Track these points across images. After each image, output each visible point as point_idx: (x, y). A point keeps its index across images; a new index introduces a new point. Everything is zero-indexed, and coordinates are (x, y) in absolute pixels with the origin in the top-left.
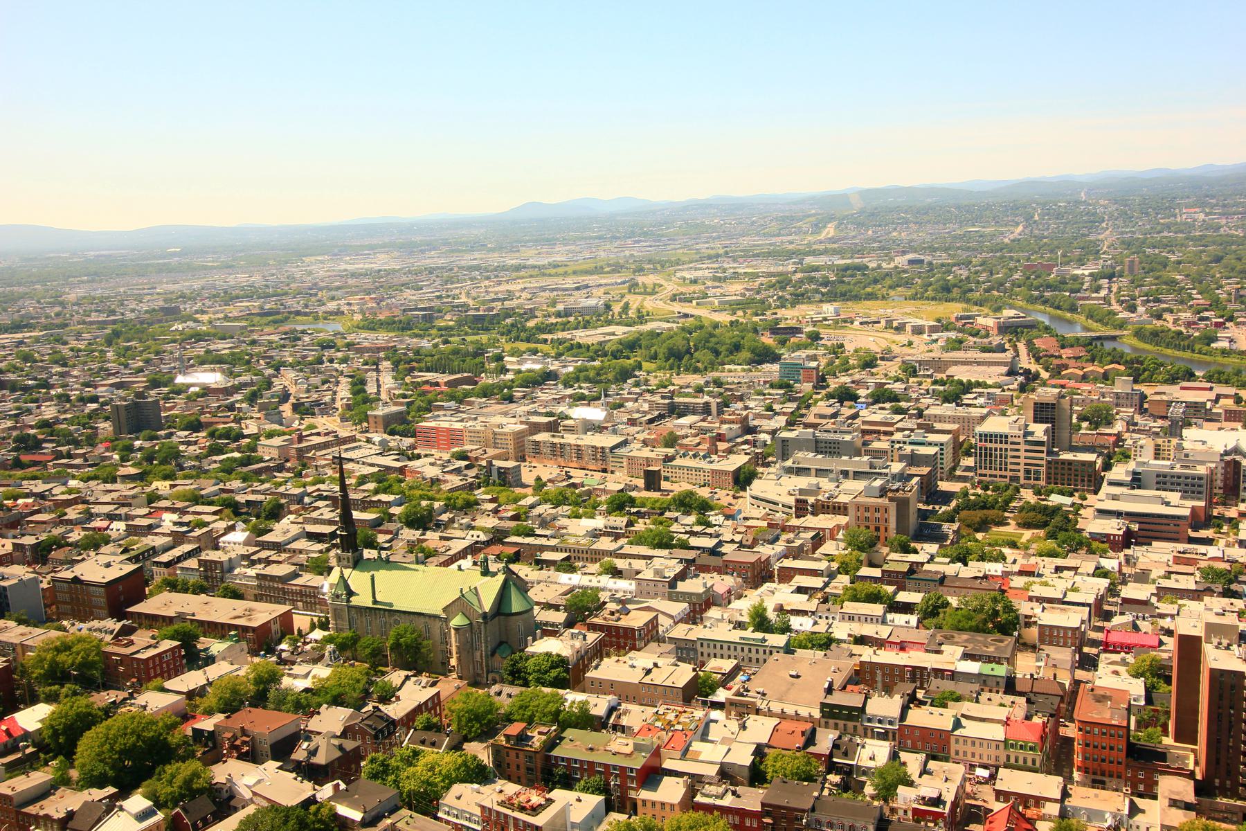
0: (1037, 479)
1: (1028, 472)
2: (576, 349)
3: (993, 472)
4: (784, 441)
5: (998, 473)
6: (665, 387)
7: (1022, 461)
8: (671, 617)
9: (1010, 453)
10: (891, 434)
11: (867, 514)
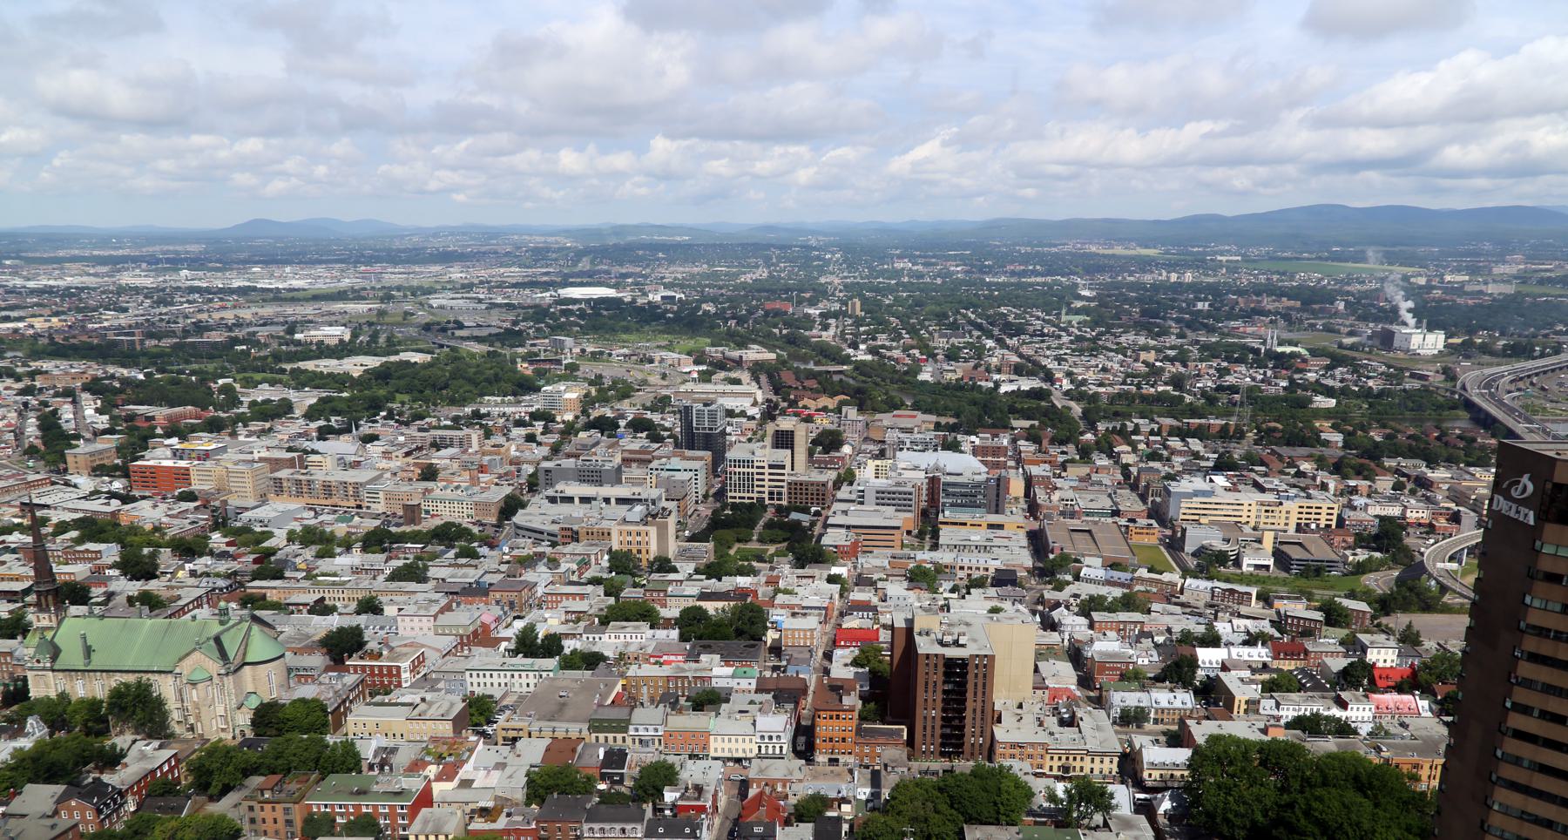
0: (779, 499)
1: (771, 493)
2: (316, 380)
3: (742, 495)
4: (548, 471)
5: (746, 495)
6: (422, 418)
7: (766, 483)
8: (438, 650)
9: (756, 477)
10: (650, 462)
11: (629, 538)
